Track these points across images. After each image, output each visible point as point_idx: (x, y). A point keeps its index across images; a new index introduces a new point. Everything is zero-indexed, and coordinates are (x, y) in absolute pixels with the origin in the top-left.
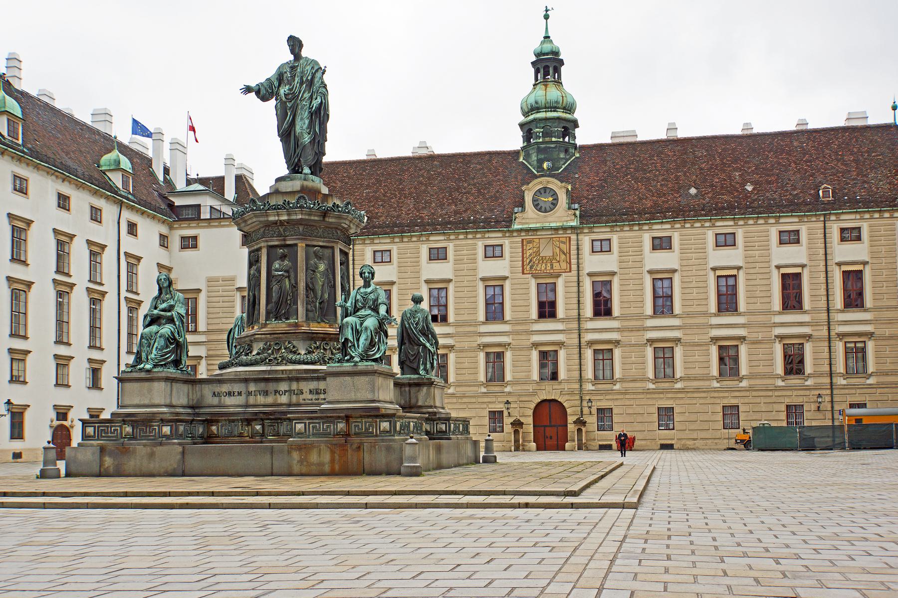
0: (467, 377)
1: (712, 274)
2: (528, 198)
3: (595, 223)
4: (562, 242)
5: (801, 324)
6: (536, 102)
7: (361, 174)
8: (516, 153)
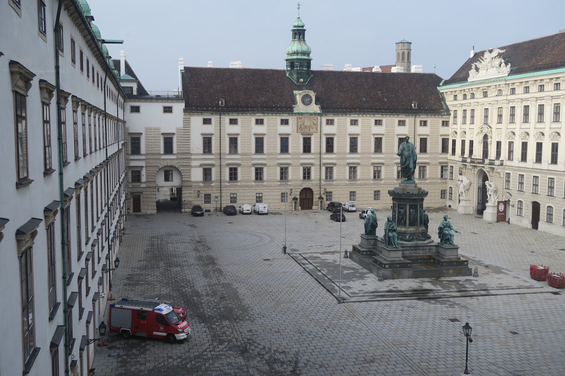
1: (372, 136)
8: (284, 72)
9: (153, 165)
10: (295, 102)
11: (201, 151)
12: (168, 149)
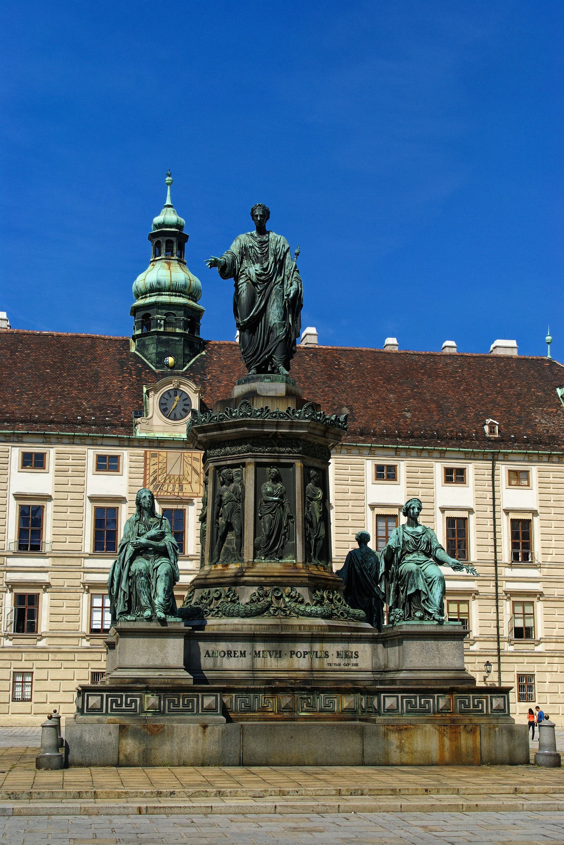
0: (64, 626)
6: (159, 283)
10: (141, 411)
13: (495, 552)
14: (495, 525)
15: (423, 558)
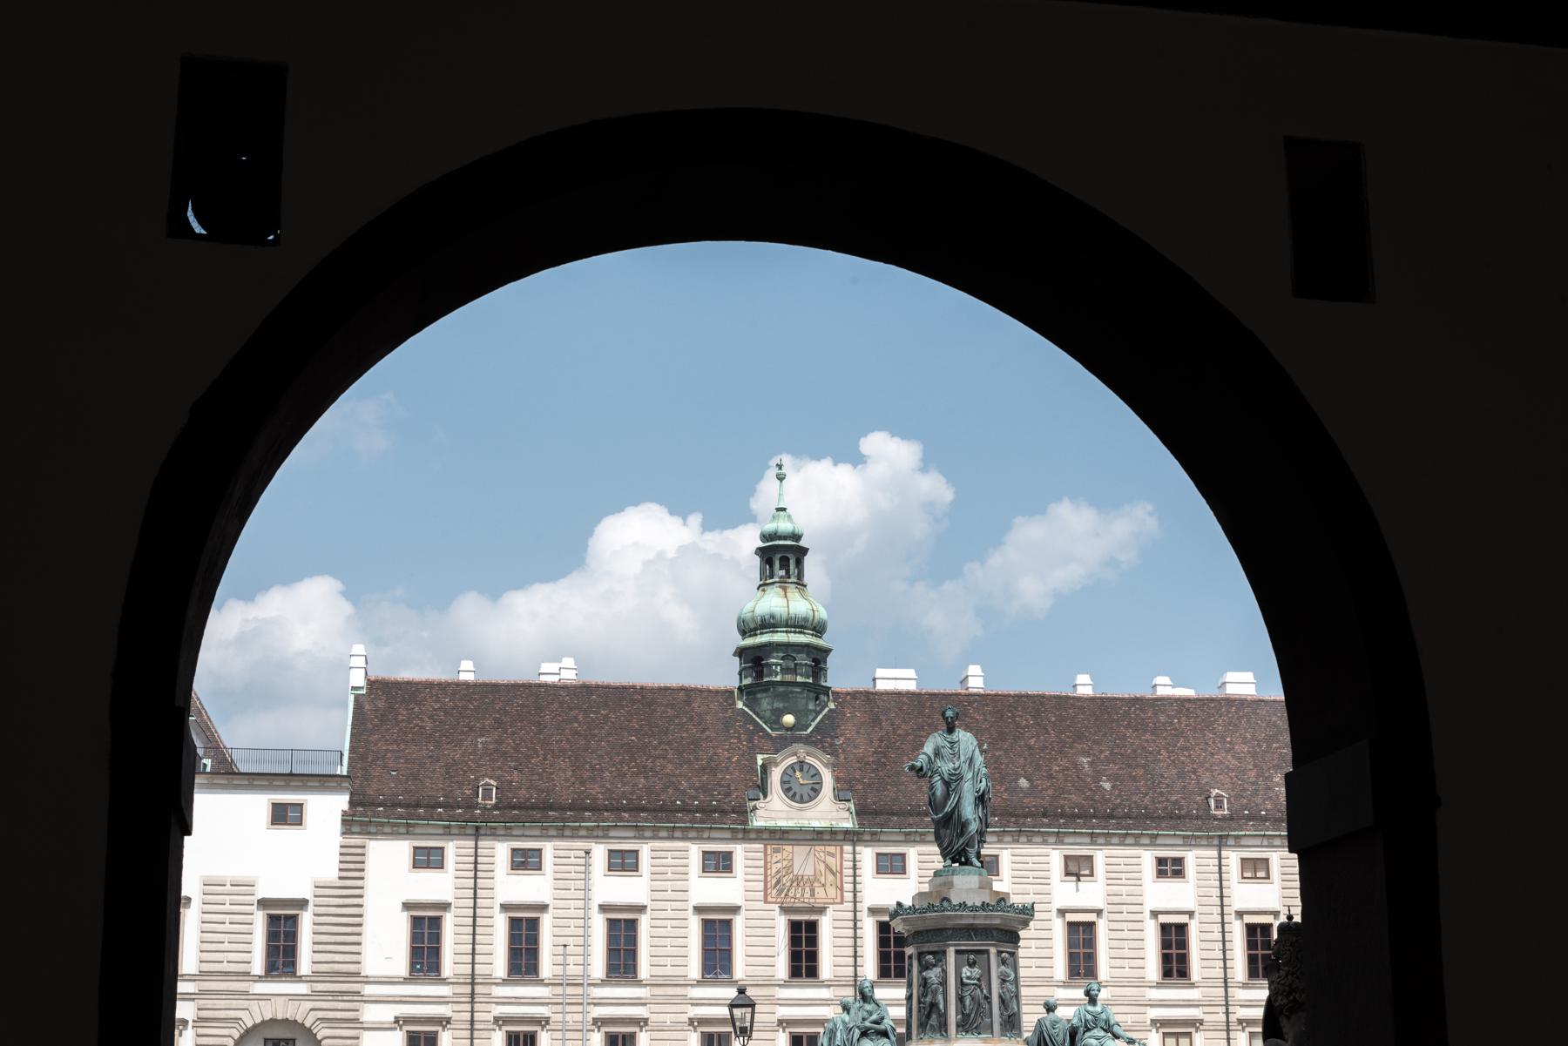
2: (776, 775)
3: (882, 826)
4: (830, 854)
5: (1189, 1004)
6: (773, 616)
7: (466, 708)
9: (221, 1014)
11: (401, 966)
12: (281, 956)
13: (1225, 968)
14: (1223, 932)
15: (1102, 1033)
